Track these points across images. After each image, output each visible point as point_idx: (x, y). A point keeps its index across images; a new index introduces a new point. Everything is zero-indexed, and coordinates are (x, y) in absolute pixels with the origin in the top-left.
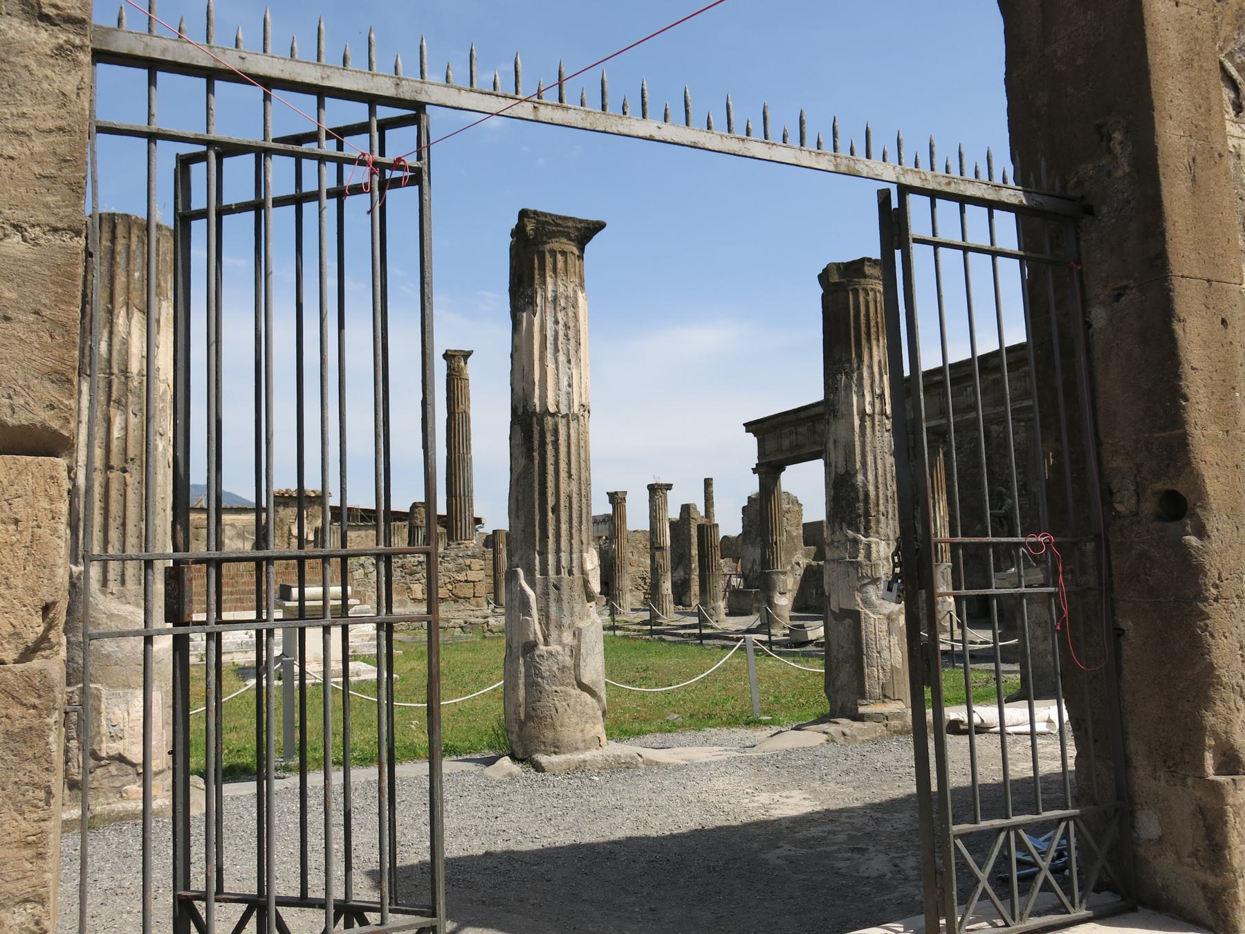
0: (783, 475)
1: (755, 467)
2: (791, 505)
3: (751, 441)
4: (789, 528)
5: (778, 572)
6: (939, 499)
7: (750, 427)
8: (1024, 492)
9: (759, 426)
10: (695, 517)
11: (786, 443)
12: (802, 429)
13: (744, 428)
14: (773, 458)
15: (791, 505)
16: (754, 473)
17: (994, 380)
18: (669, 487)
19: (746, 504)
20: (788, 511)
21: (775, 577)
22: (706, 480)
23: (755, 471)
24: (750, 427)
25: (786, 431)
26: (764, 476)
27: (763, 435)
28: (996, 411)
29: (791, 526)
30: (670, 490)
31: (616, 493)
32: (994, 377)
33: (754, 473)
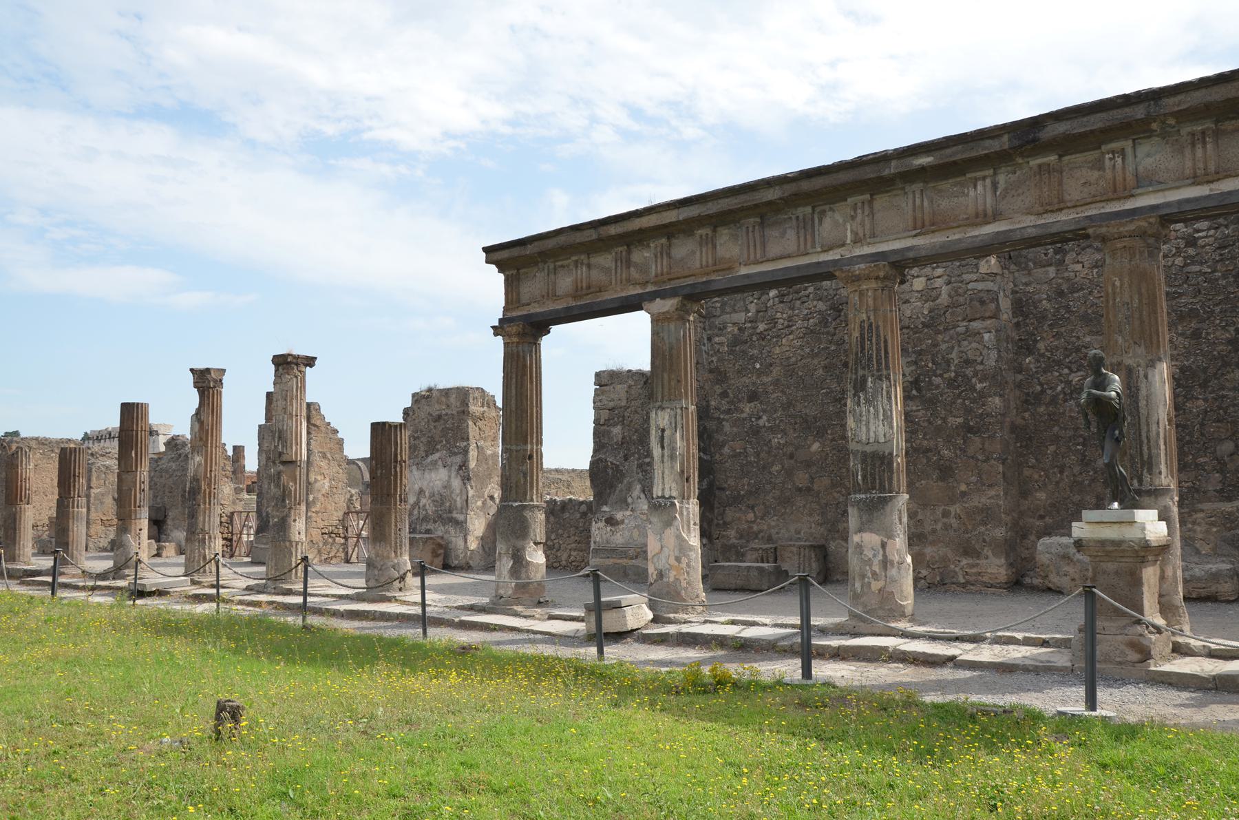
0: (545, 341)
1: (497, 324)
2: (485, 409)
3: (493, 282)
4: (481, 443)
5: (534, 506)
6: (895, 381)
7: (494, 254)
8: (914, 392)
9: (515, 252)
10: (318, 423)
11: (565, 282)
12: (605, 260)
13: (484, 254)
14: (535, 309)
15: (485, 408)
16: (496, 334)
17: (1040, 166)
18: (310, 361)
19: (409, 405)
20: (482, 417)
21: (528, 514)
22: (268, 393)
23: (497, 330)
24: (494, 254)
25: (565, 263)
26: (515, 340)
27: (518, 270)
28: (1043, 221)
29: (485, 439)
30: (311, 366)
31: (208, 370)
32: (1039, 161)
33: (496, 334)
